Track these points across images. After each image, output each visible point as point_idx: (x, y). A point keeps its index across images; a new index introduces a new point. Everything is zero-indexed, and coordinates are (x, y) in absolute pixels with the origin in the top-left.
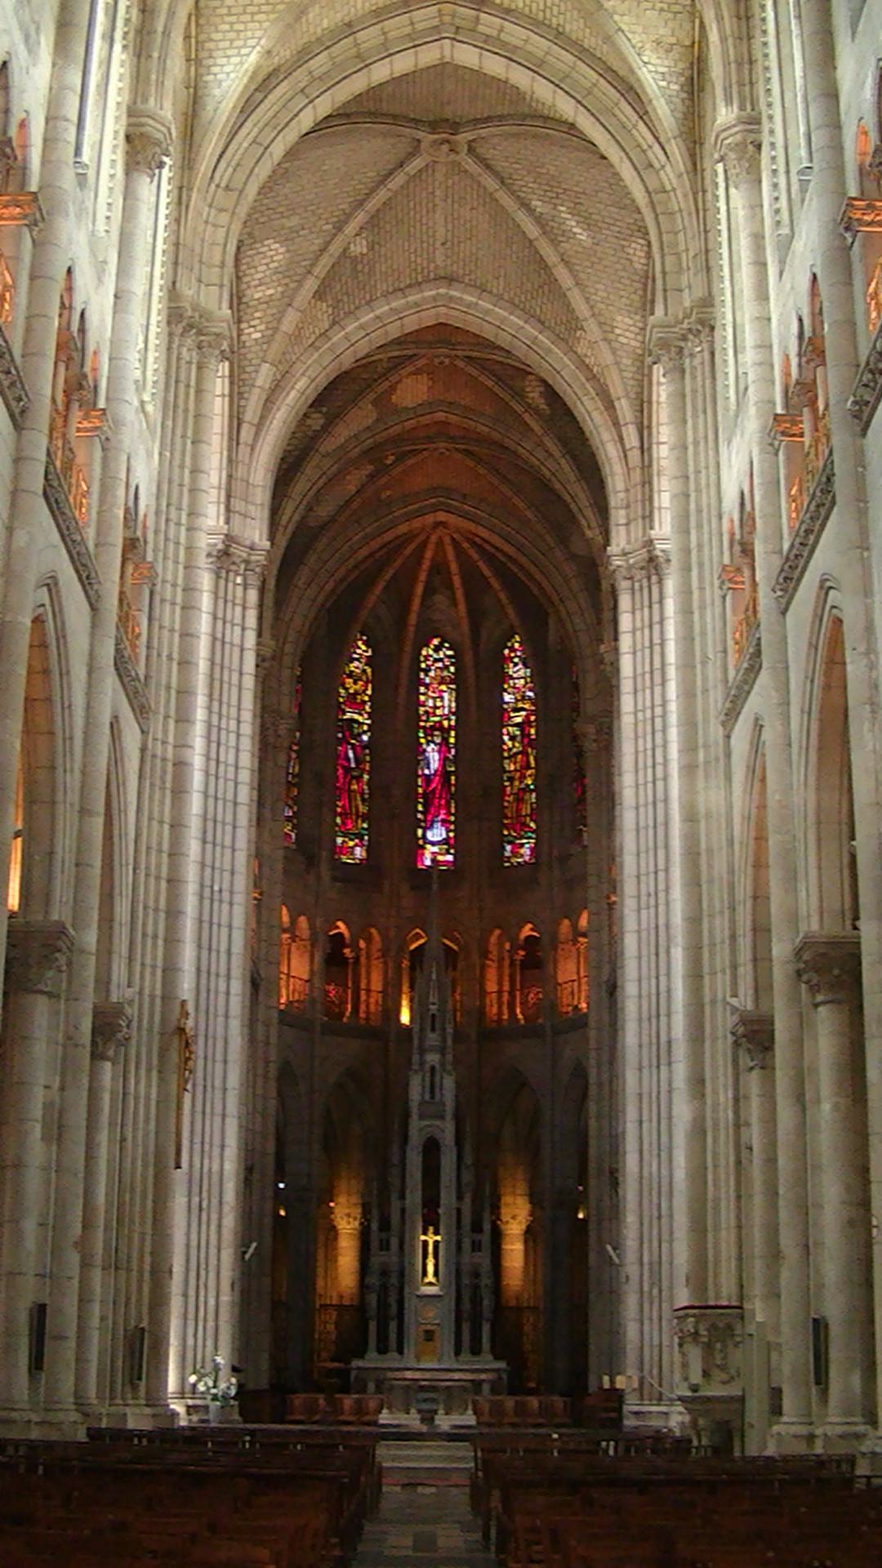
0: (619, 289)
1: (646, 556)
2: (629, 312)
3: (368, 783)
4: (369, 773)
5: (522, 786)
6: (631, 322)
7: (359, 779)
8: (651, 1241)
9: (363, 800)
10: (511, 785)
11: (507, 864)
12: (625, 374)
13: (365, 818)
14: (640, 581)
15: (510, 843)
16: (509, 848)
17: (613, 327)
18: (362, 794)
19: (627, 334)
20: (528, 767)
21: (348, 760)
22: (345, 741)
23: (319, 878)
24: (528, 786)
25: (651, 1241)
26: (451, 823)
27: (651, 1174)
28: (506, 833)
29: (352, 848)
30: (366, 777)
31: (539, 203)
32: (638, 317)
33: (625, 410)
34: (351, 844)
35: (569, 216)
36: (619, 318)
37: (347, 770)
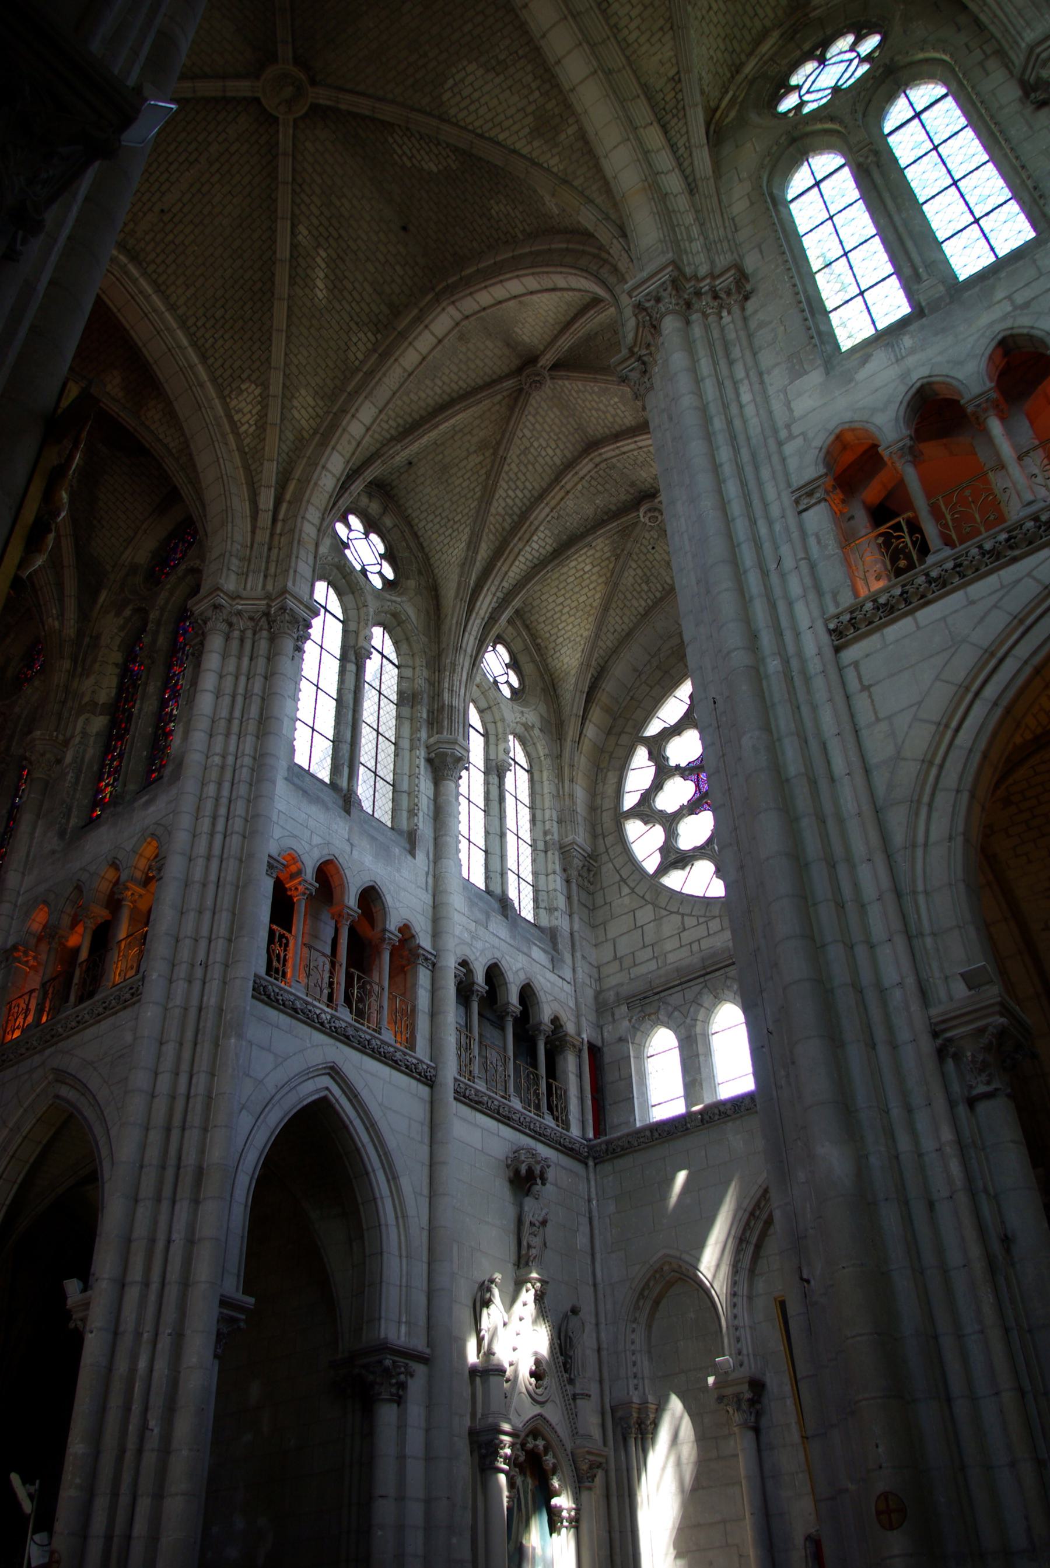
0: (319, 365)
1: (263, 608)
2: (317, 393)
6: (312, 403)
8: (115, 1494)
12: (284, 447)
14: (243, 632)
17: (293, 396)
19: (303, 411)
25: (115, 1494)
27: (133, 1371)
31: (305, 232)
32: (321, 404)
33: (270, 472)
35: (323, 266)
36: (303, 392)
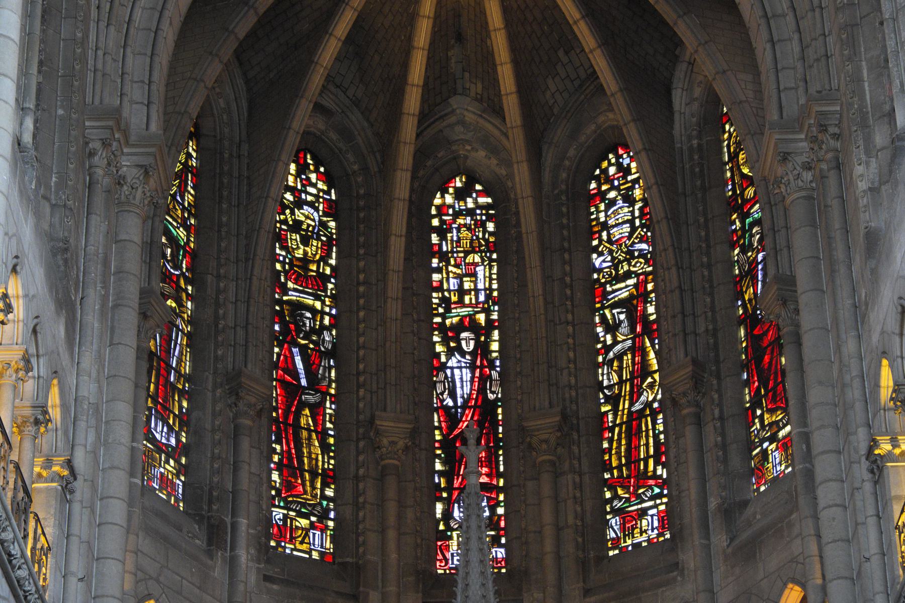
3: (337, 419)
4: (335, 399)
5: (637, 407)
7: (317, 410)
9: (325, 448)
10: (615, 410)
11: (611, 553)
13: (328, 478)
15: (616, 512)
16: (615, 522)
18: (323, 435)
20: (644, 371)
21: (296, 376)
22: (287, 339)
23: (233, 562)
24: (648, 404)
26: (499, 490)
28: (608, 495)
29: (307, 530)
30: (330, 408)
34: (304, 522)
37: (292, 390)
